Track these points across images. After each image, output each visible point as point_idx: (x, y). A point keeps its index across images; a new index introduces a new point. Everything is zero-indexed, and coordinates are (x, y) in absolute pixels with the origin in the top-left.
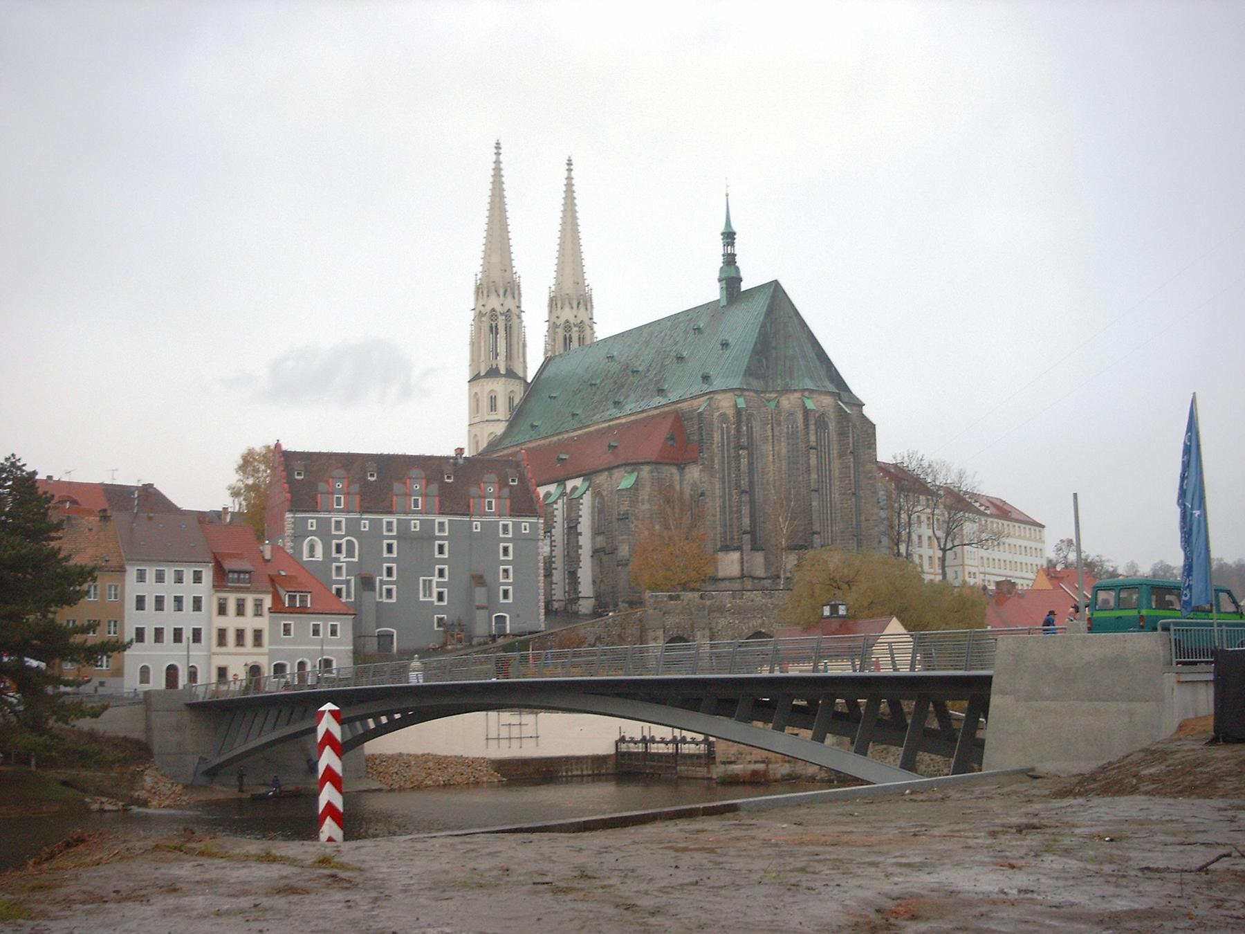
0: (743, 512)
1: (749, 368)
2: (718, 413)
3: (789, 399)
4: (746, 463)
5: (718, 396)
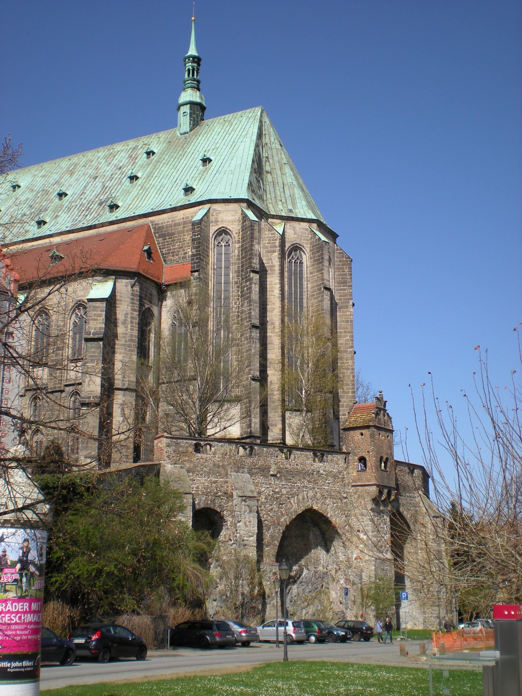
0: (253, 351)
1: (251, 183)
2: (216, 228)
3: (294, 228)
4: (257, 289)
5: (215, 206)
